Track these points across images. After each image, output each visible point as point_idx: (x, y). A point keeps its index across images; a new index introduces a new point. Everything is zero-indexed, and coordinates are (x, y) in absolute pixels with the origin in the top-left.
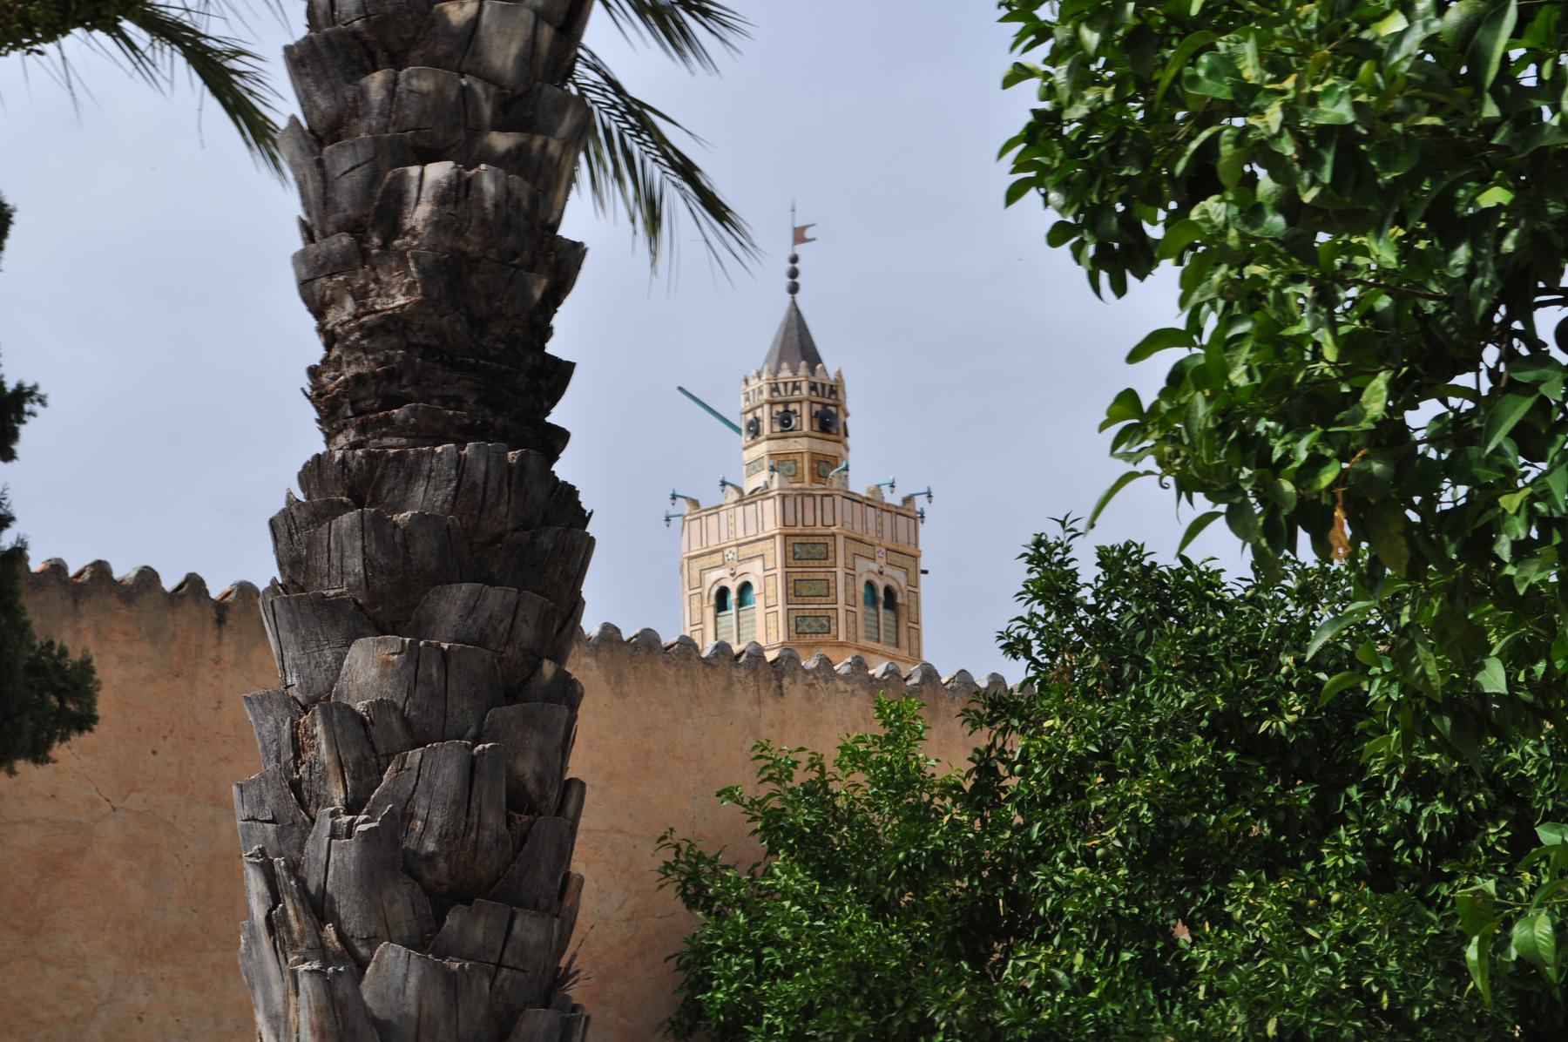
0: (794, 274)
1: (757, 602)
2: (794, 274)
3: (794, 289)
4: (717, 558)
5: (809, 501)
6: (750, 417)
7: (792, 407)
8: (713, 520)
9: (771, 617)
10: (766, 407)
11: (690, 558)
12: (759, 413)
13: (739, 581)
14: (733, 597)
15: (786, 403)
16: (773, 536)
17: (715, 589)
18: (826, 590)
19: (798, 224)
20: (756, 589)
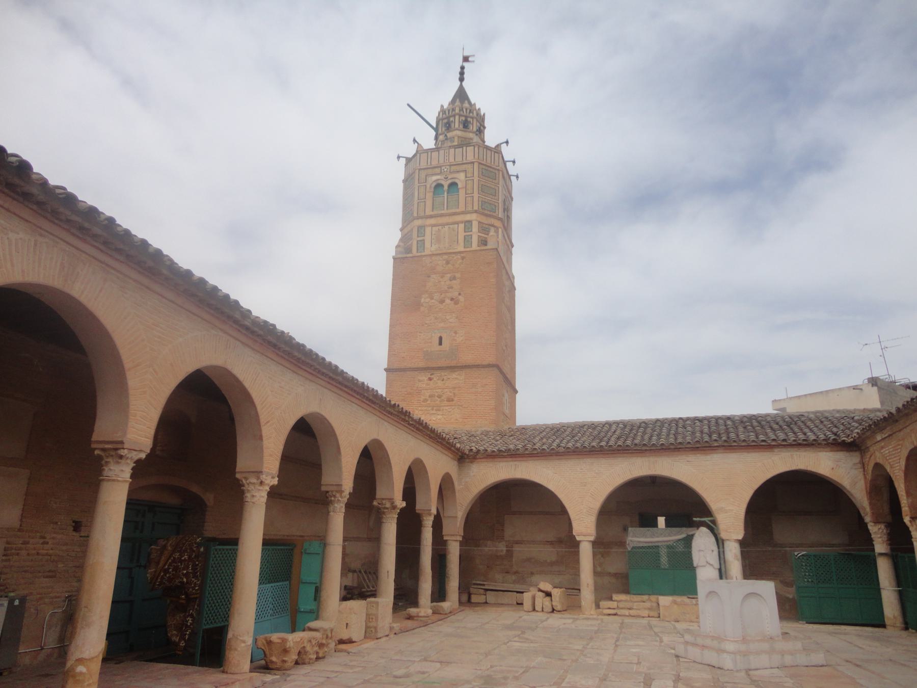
0: (462, 73)
1: (462, 193)
2: (462, 73)
3: (462, 79)
4: (438, 170)
5: (489, 152)
6: (446, 121)
7: (469, 119)
8: (435, 154)
9: (469, 199)
10: (457, 117)
11: (420, 170)
12: (452, 119)
13: (450, 181)
14: (446, 188)
15: (466, 117)
16: (473, 163)
17: (434, 184)
18: (495, 194)
19: (466, 54)
20: (460, 186)
